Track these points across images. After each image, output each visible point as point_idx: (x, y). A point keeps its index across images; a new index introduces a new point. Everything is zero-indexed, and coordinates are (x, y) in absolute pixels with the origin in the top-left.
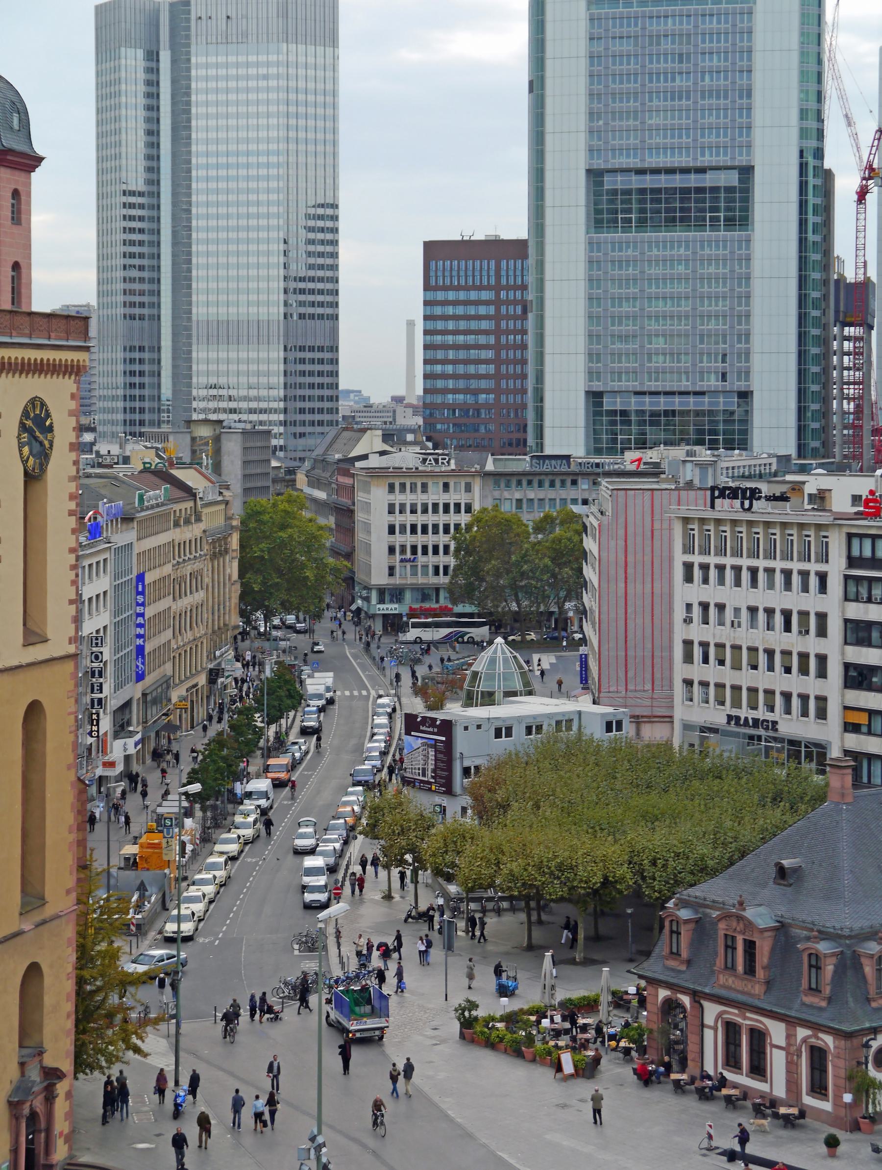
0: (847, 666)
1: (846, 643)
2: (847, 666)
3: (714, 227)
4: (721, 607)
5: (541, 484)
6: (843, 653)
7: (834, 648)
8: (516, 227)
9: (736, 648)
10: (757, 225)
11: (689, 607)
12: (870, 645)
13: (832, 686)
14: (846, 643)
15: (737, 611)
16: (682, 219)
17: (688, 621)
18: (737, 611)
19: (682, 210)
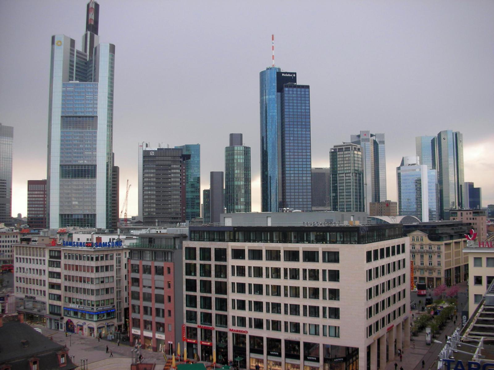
0: (50, 283)
1: (49, 277)
2: (50, 283)
3: (88, 178)
4: (24, 268)
5: (14, 236)
6: (48, 279)
7: (46, 277)
8: (45, 178)
9: (27, 279)
10: (97, 178)
11: (17, 268)
12: (54, 277)
13: (46, 288)
14: (49, 277)
15: (27, 269)
16: (81, 176)
17: (17, 272)
18: (27, 269)
19: (81, 174)
